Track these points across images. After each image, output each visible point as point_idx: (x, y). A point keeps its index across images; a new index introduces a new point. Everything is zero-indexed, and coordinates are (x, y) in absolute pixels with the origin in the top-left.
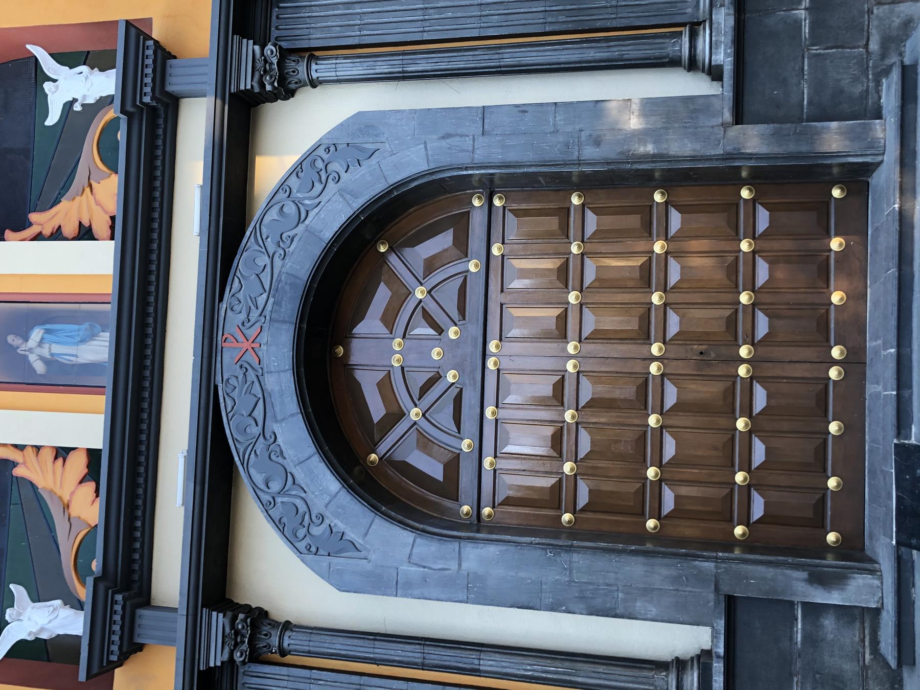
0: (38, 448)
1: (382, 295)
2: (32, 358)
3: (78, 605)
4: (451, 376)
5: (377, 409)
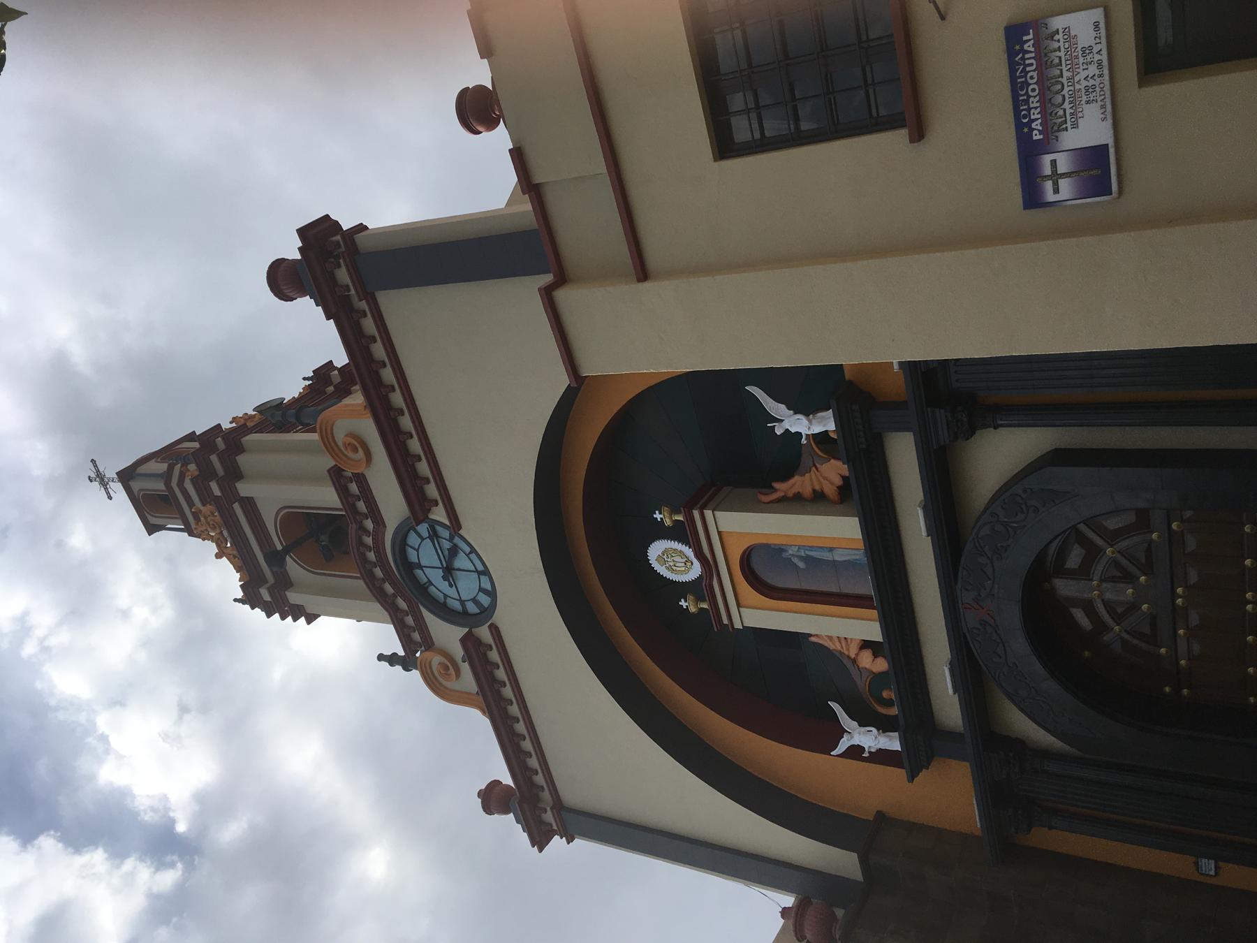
2: (795, 560)
3: (885, 725)
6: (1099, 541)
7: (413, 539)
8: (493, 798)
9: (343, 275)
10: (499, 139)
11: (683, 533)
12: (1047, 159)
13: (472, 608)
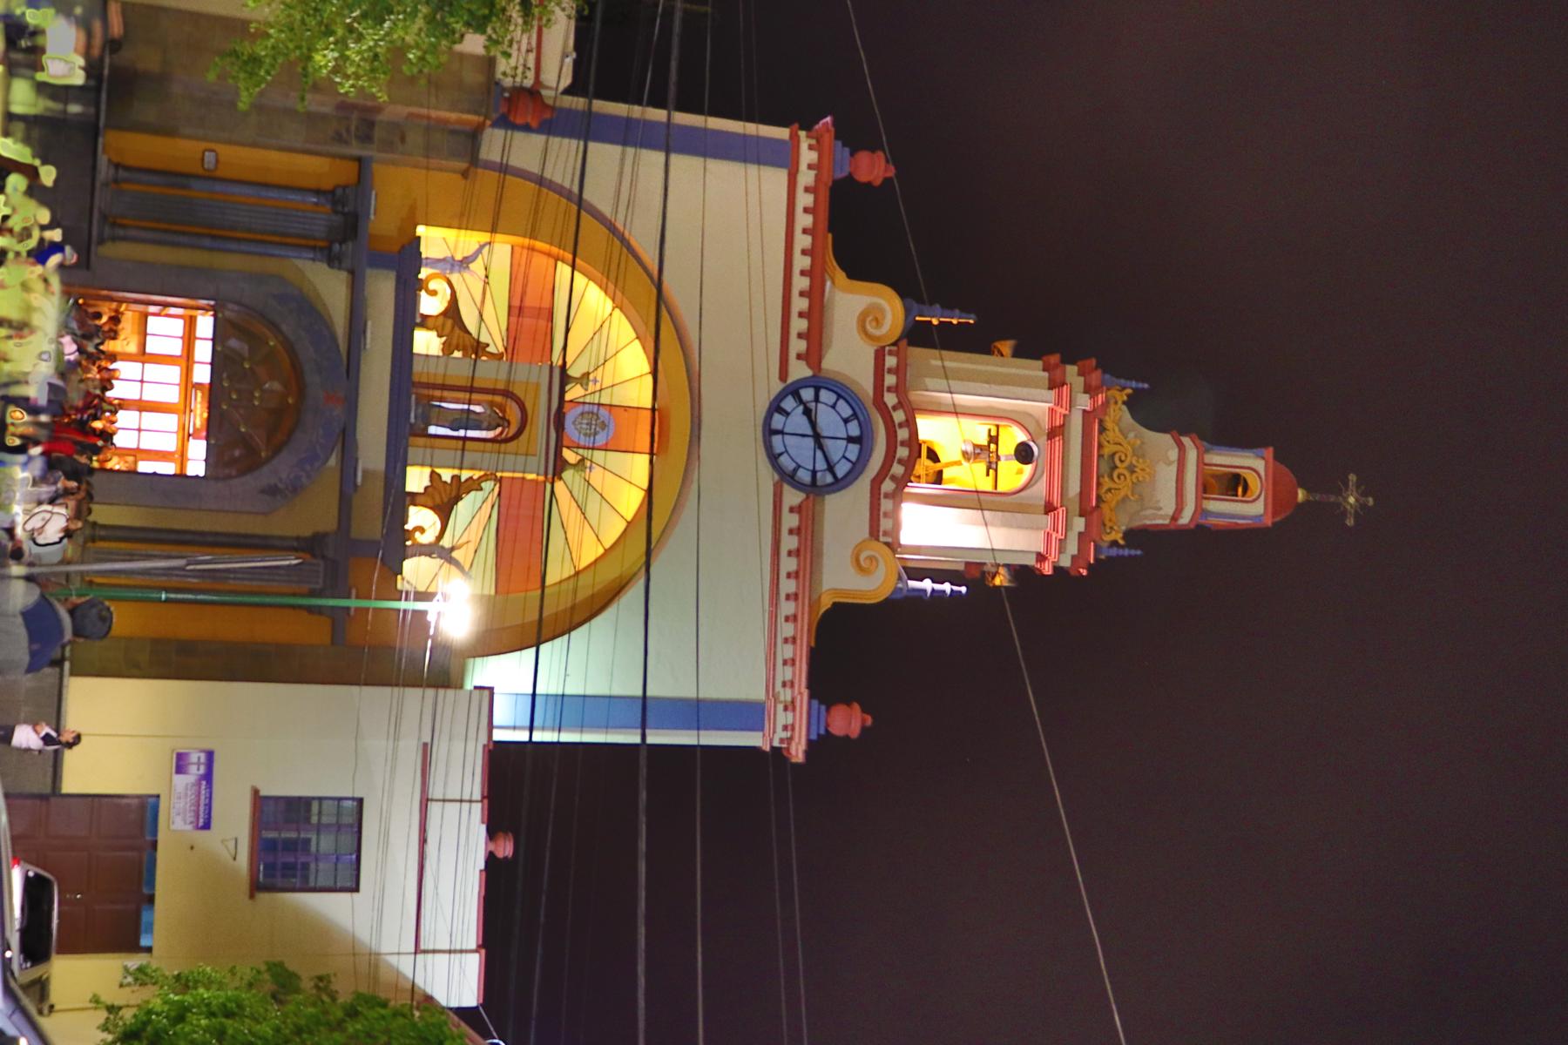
7: (842, 469)
12: (202, 770)
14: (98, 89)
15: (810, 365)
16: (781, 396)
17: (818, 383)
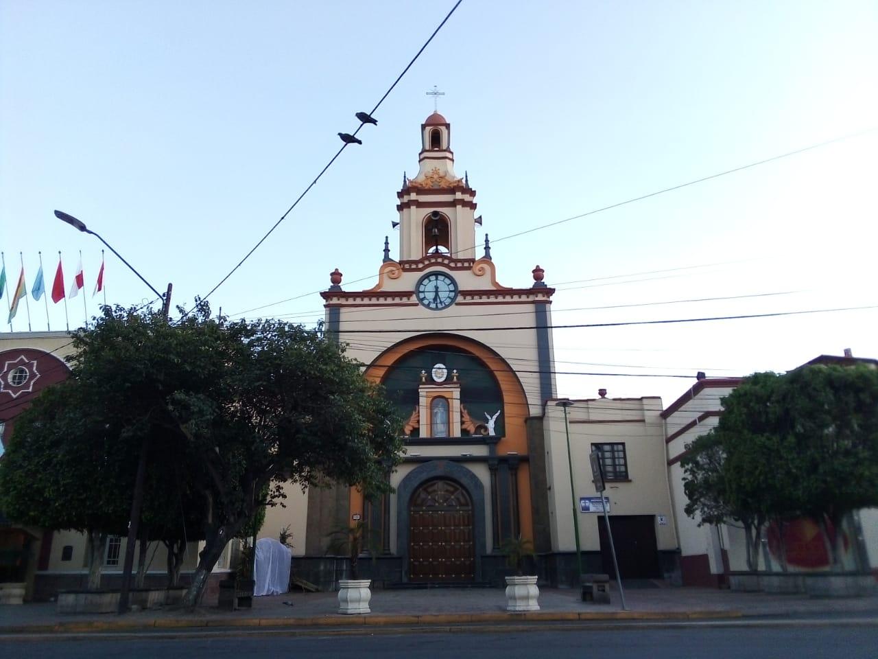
0: (419, 416)
1: (452, 489)
4: (437, 504)
5: (430, 490)
6: (456, 494)
7: (448, 281)
8: (336, 277)
9: (540, 298)
10: (598, 397)
11: (449, 380)
13: (422, 296)
14: (337, 559)
15: (411, 295)
16: (424, 305)
17: (417, 292)
